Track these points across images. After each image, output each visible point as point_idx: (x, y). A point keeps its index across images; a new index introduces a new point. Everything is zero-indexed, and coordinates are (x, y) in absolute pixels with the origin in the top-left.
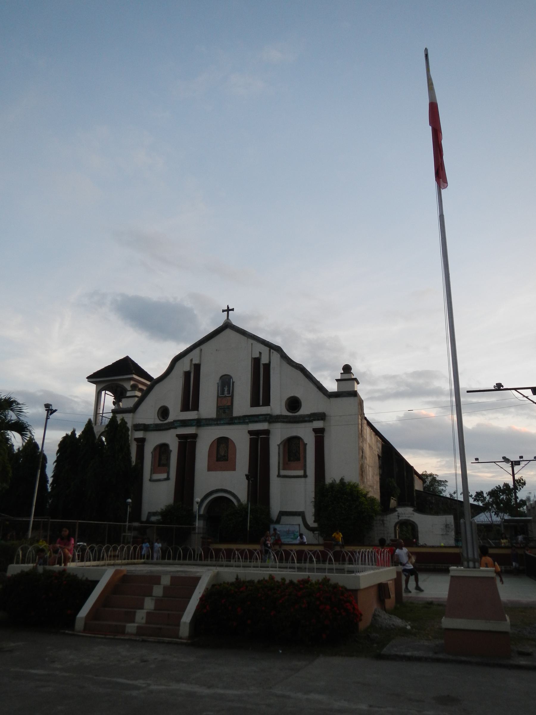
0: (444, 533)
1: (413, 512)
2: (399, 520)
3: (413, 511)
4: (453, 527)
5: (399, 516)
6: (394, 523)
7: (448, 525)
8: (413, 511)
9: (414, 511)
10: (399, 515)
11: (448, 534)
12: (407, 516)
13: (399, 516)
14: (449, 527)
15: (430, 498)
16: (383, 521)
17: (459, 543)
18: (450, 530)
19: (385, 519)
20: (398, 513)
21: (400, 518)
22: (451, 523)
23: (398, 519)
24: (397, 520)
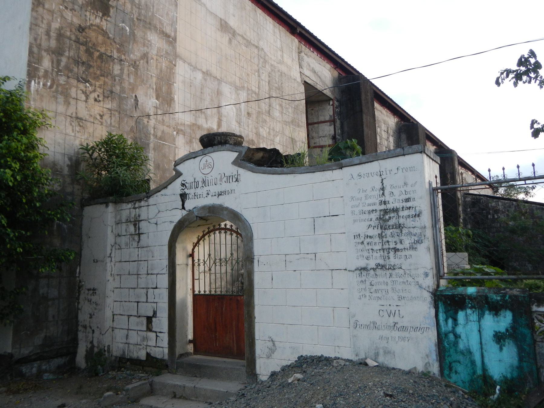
0: (372, 264)
1: (234, 170)
2: (184, 213)
3: (235, 163)
4: (426, 219)
5: (183, 197)
6: (172, 226)
7: (396, 210)
8: (235, 163)
9: (240, 166)
10: (187, 191)
11: (393, 268)
12: (214, 189)
13: (183, 197)
14: (400, 227)
15: (494, 204)
16: (136, 222)
17: (461, 315)
18: (407, 242)
19: (144, 213)
20: (183, 185)
21: (190, 204)
22: (408, 200)
23: (183, 208)
24: (179, 215)
